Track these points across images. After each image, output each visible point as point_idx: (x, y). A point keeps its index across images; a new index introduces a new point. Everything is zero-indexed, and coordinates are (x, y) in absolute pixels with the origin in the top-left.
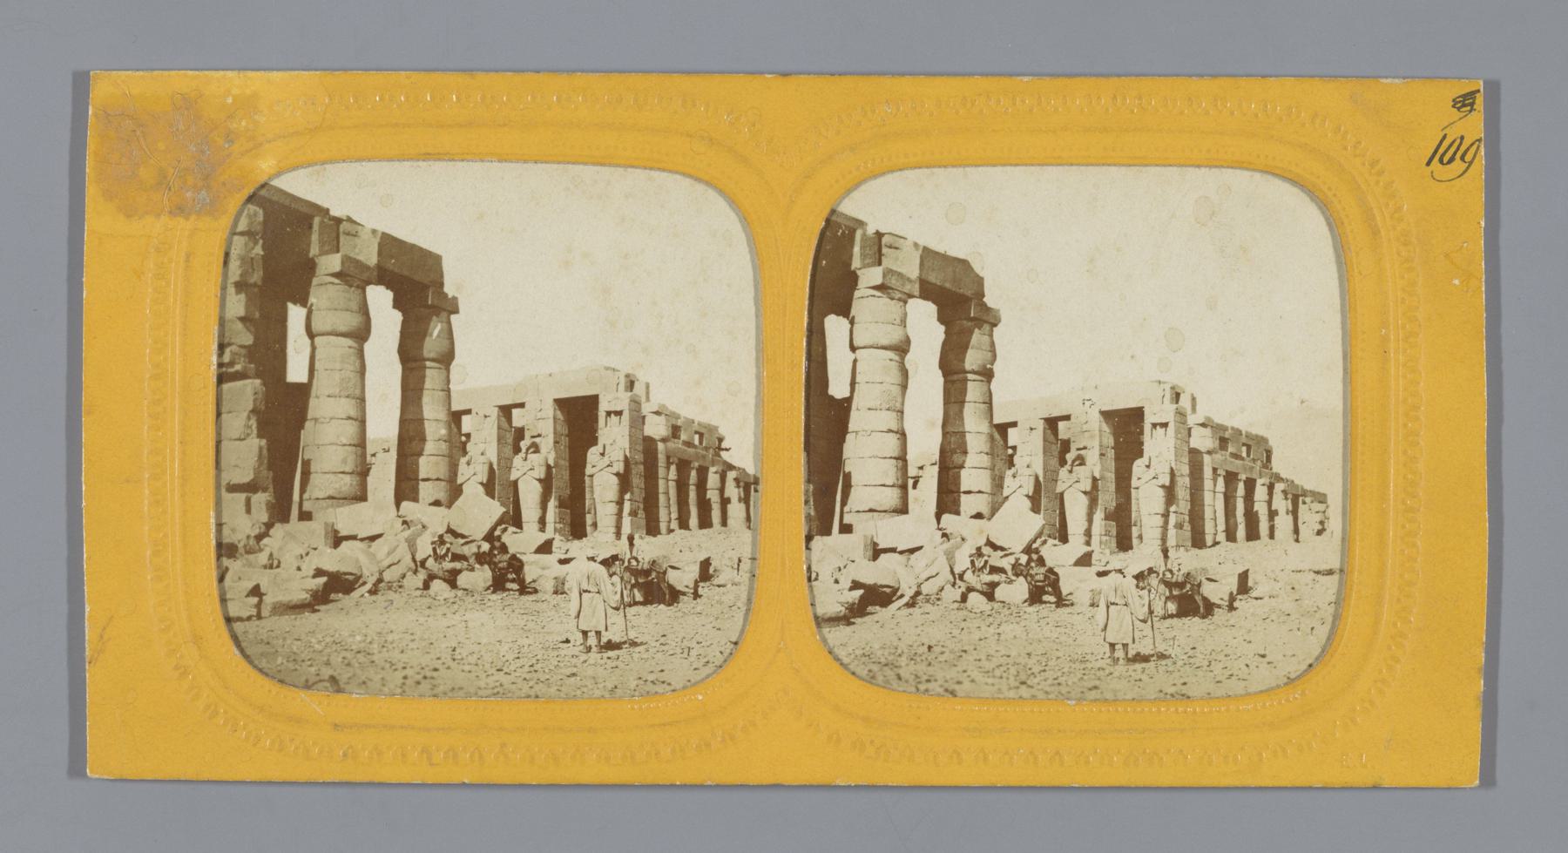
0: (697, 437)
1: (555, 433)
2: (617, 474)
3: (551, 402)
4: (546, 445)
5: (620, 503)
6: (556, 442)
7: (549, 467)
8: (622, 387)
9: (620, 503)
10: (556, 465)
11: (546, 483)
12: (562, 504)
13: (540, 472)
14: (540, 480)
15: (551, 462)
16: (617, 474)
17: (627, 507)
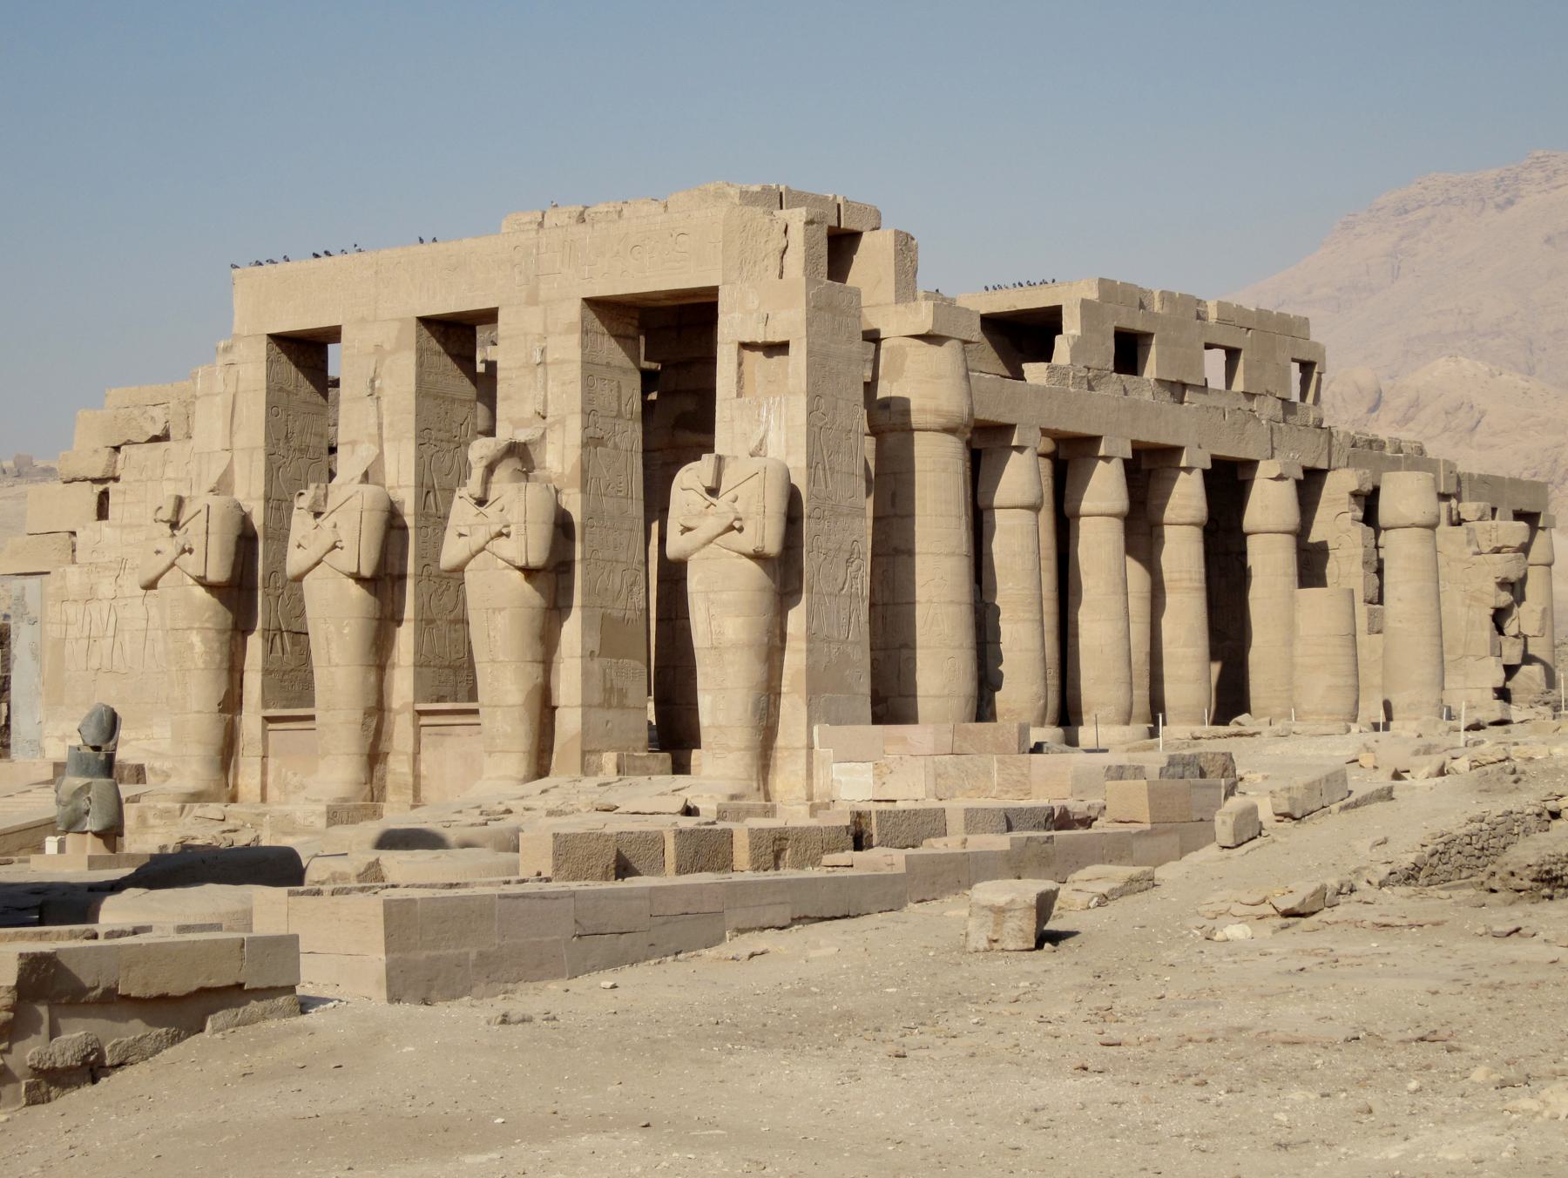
0: (1216, 359)
1: (588, 413)
2: (757, 557)
3: (573, 311)
4: (560, 456)
5: (773, 648)
6: (591, 442)
7: (563, 527)
8: (795, 262)
9: (773, 648)
10: (588, 516)
11: (552, 576)
12: (608, 639)
13: (532, 546)
14: (529, 572)
15: (573, 503)
16: (757, 557)
17: (795, 659)
